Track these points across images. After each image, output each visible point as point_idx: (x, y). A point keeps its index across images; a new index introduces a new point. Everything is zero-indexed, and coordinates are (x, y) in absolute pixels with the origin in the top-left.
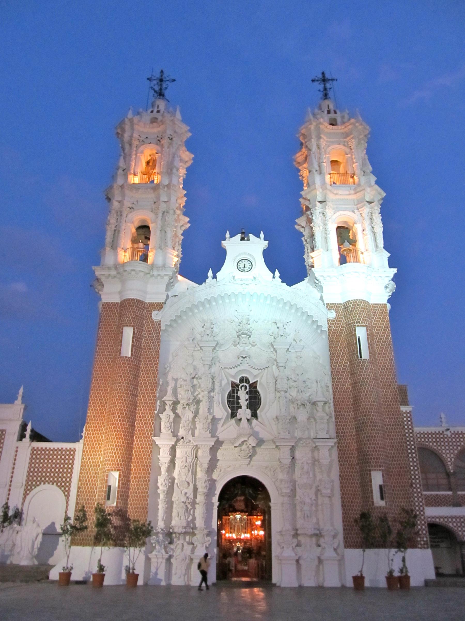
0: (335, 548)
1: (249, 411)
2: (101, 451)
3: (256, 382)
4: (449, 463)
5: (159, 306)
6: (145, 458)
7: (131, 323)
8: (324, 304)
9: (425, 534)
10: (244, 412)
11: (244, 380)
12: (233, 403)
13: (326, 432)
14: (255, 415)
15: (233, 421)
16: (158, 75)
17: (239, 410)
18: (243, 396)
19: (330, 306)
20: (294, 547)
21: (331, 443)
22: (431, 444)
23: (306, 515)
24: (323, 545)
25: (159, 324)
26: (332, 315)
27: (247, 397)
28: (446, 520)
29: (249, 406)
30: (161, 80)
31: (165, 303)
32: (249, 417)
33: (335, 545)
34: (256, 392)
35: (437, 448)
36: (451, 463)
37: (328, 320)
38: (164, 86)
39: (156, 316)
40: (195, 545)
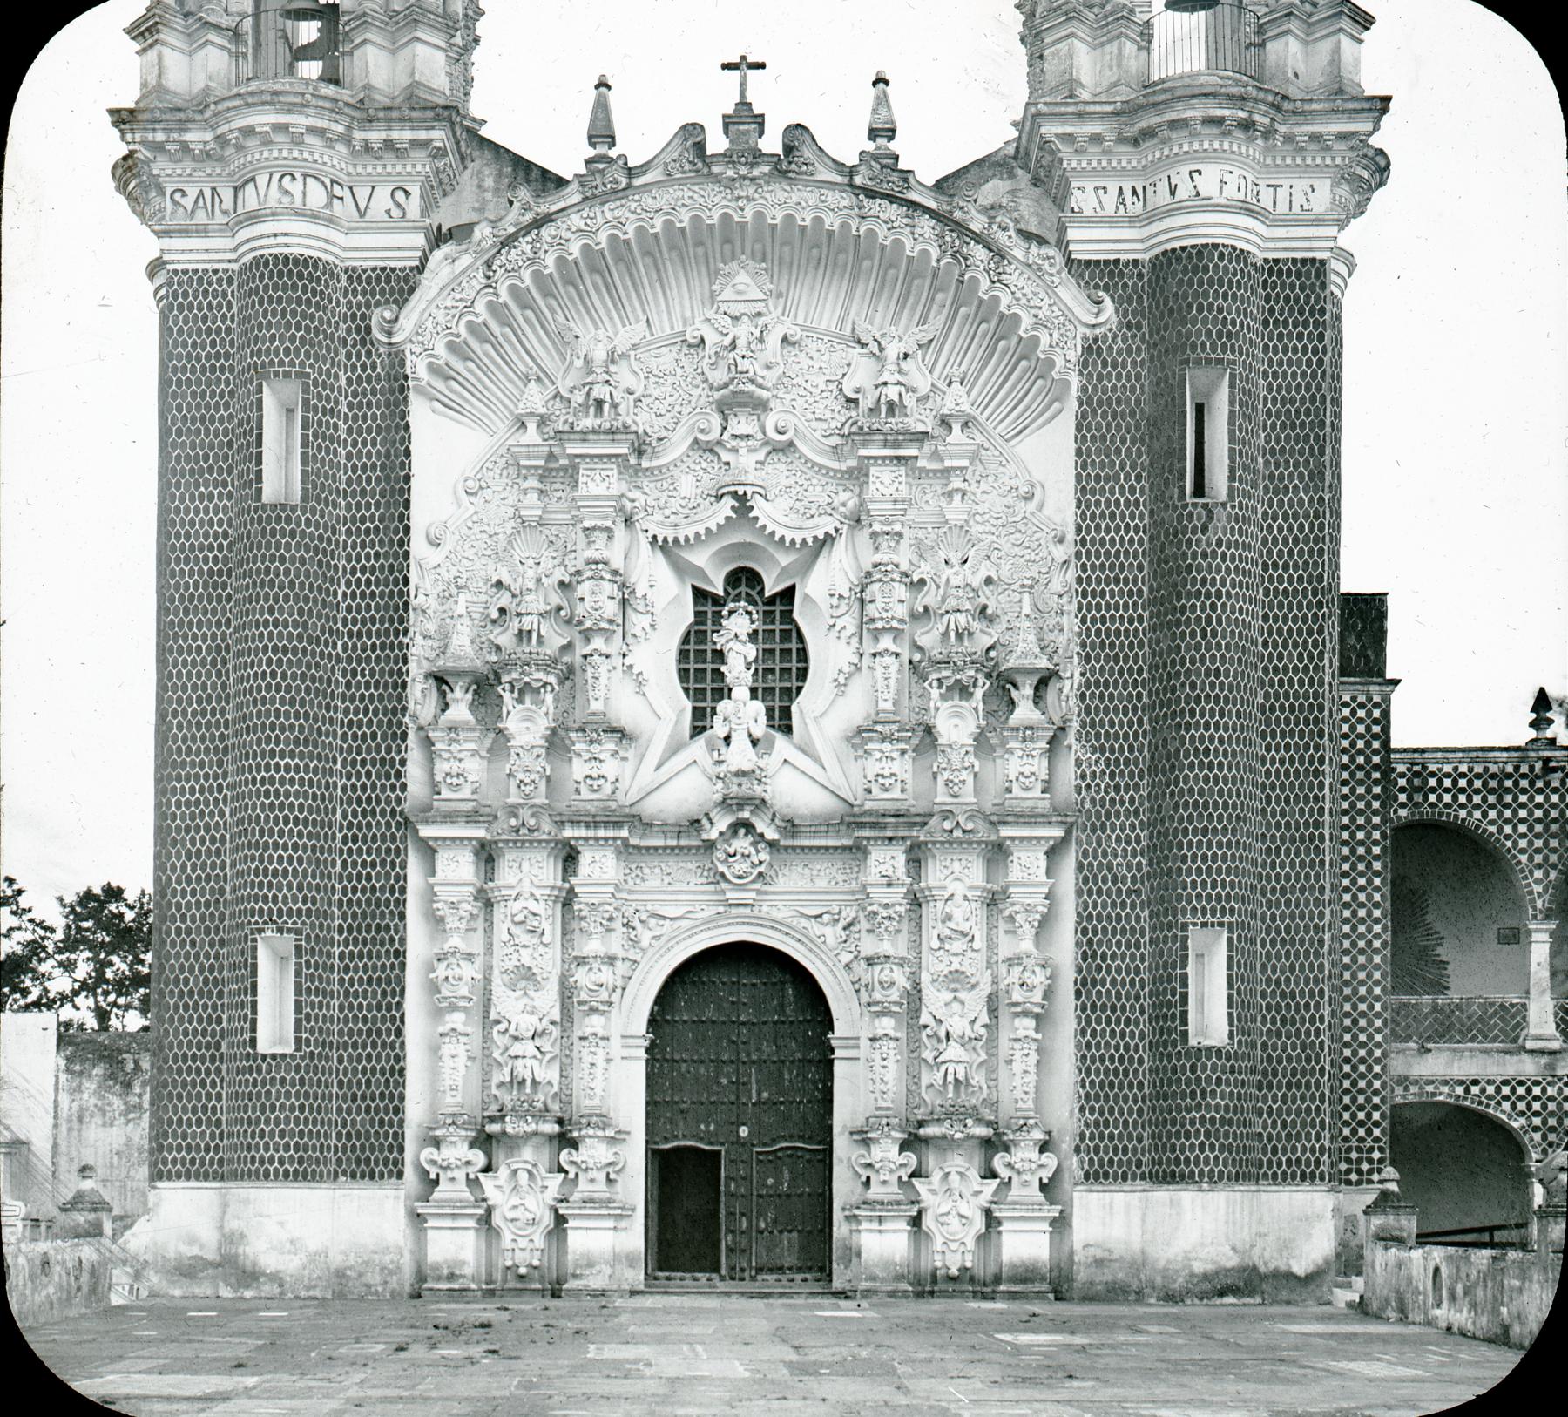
0: (1045, 1181)
1: (758, 707)
2: (223, 868)
4: (1538, 888)
6: (383, 888)
7: (292, 364)
8: (1069, 262)
9: (1377, 1140)
10: (743, 711)
12: (701, 675)
13: (1039, 786)
14: (781, 721)
15: (701, 740)
17: (723, 706)
20: (905, 1178)
22: (1477, 814)
23: (950, 1078)
24: (1004, 1173)
27: (751, 651)
28: (1475, 1090)
31: (421, 268)
32: (760, 729)
33: (1046, 1175)
35: (1500, 830)
36: (1546, 889)
40: (571, 1176)
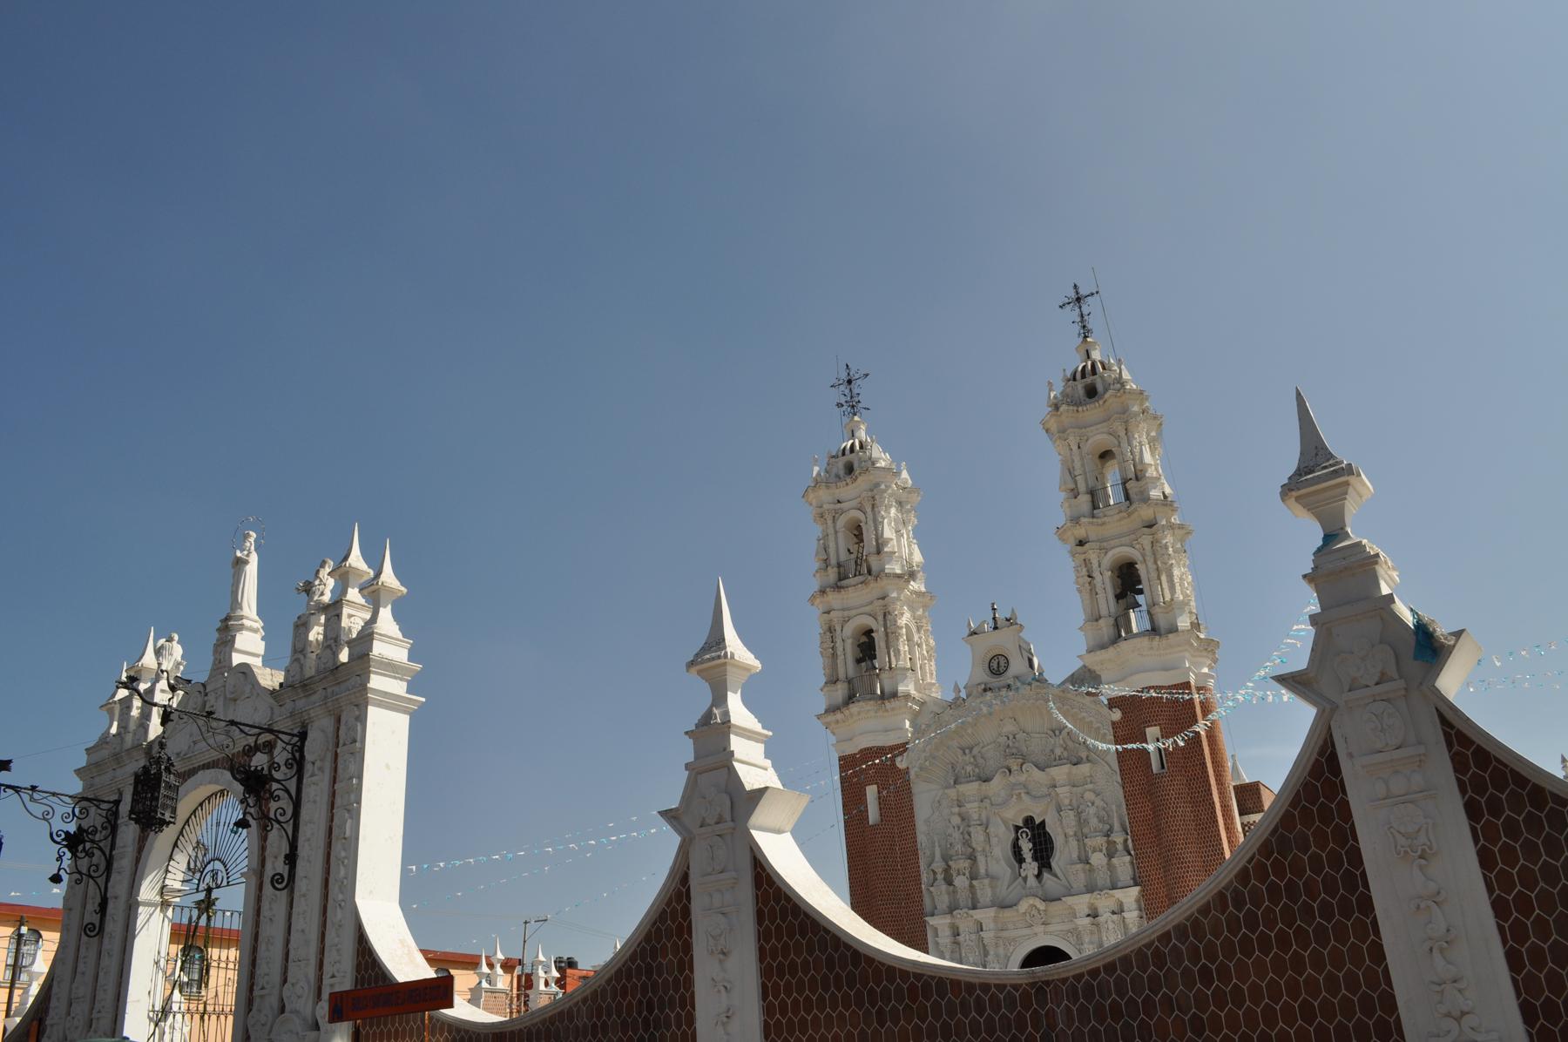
1: (1035, 865)
3: (1043, 822)
5: (902, 748)
10: (1031, 867)
11: (1029, 821)
16: (844, 376)
18: (1026, 846)
19: (1114, 703)
21: (1135, 891)
25: (907, 771)
26: (1117, 715)
29: (1035, 858)
30: (850, 382)
34: (1046, 834)
37: (1113, 723)
38: (855, 391)
39: (901, 763)
